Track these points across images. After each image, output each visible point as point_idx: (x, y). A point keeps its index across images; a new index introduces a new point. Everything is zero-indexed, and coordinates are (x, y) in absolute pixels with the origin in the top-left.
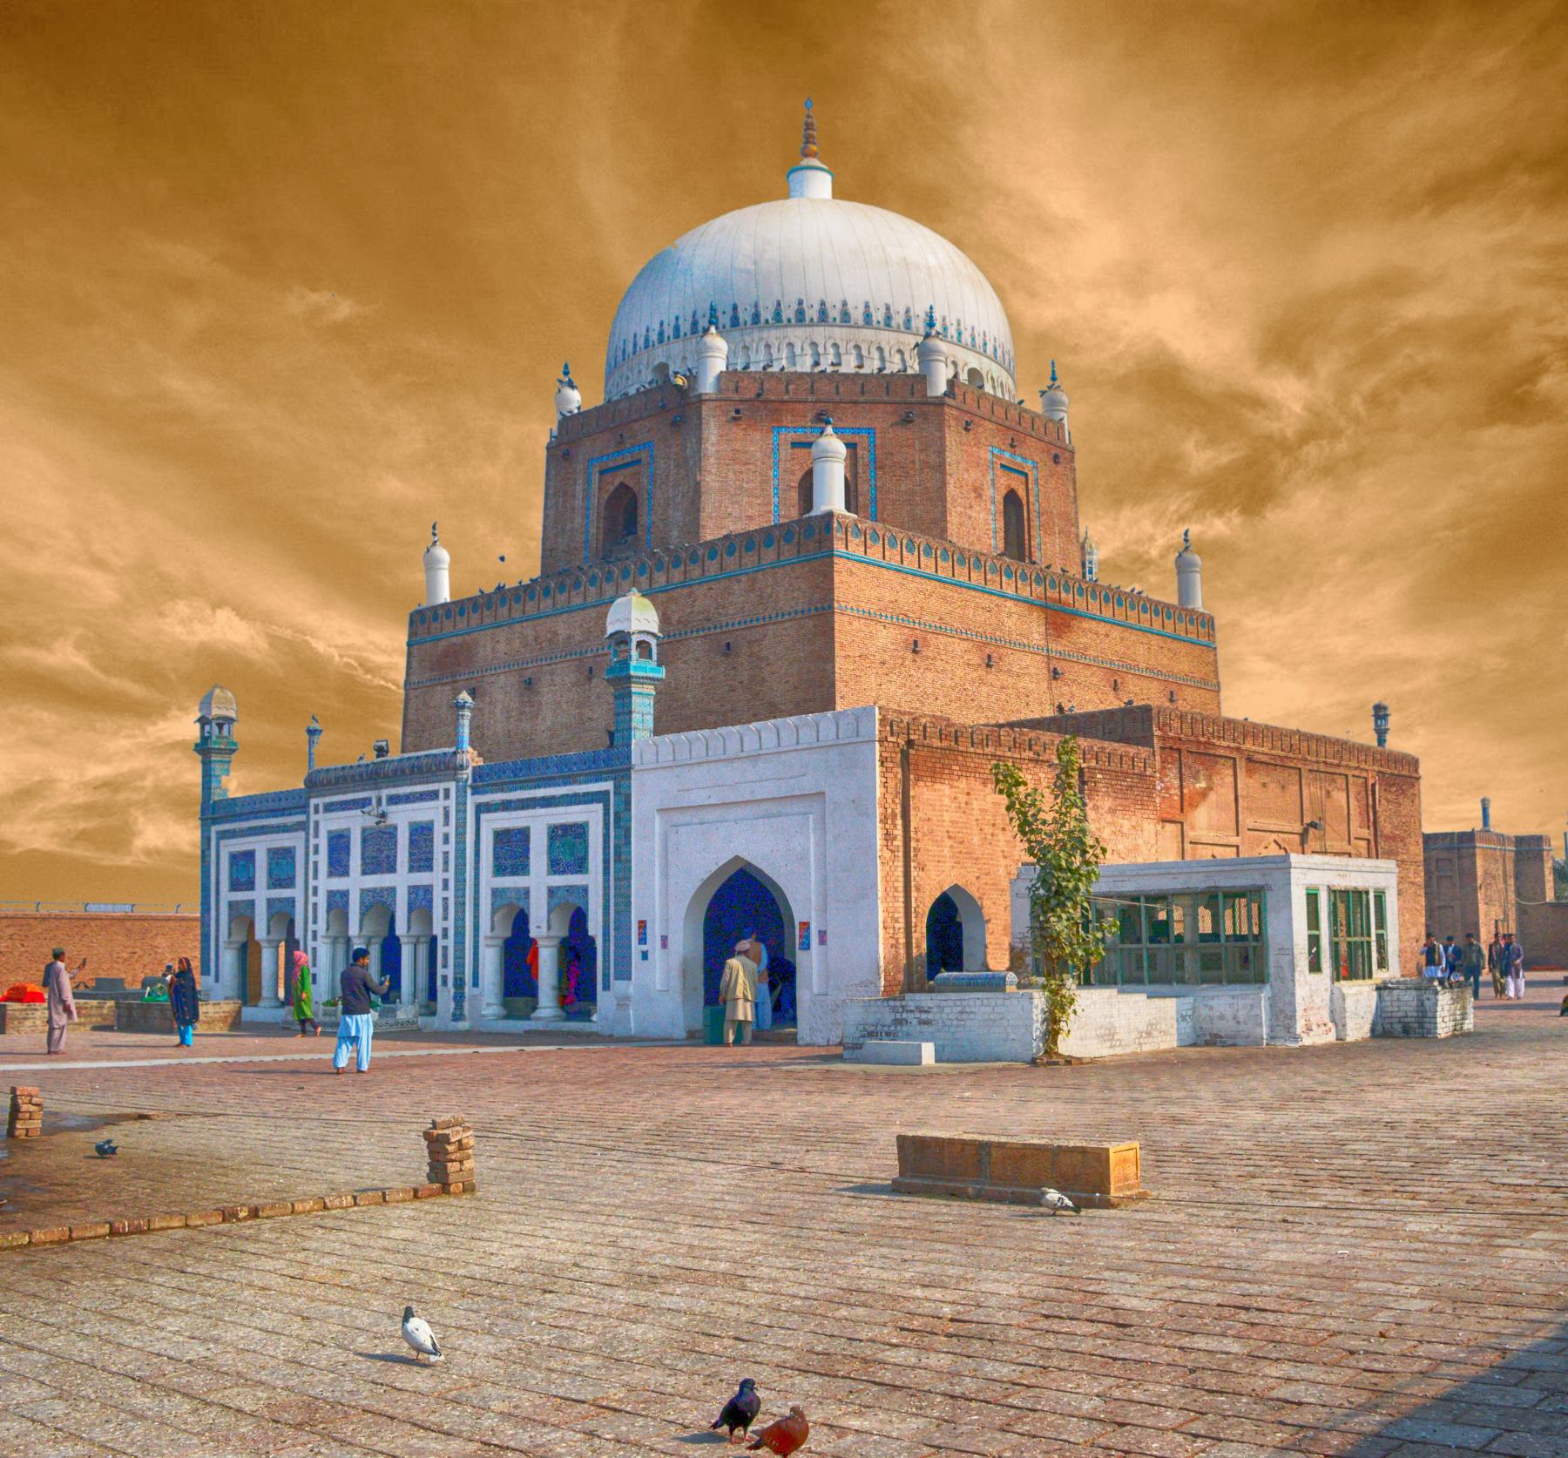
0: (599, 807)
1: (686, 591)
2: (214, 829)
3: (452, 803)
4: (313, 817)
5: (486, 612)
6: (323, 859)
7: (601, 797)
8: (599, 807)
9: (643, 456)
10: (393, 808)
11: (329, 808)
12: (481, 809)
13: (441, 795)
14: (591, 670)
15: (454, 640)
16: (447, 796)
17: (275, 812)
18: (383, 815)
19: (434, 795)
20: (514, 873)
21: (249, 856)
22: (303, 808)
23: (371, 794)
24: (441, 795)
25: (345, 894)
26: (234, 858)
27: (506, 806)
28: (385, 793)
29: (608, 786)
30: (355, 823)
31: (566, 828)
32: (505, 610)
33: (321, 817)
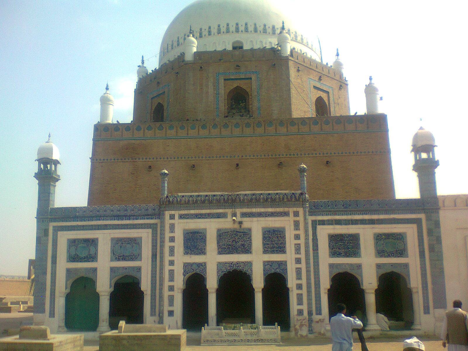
0: (415, 226)
1: (299, 136)
2: (52, 224)
3: (301, 218)
4: (168, 221)
5: (158, 131)
6: (179, 244)
7: (418, 222)
8: (415, 226)
9: (254, 78)
10: (245, 219)
11: (181, 217)
12: (315, 224)
13: (291, 214)
14: (237, 165)
15: (133, 141)
16: (296, 214)
17: (118, 217)
18: (240, 223)
19: (286, 214)
20: (347, 255)
21: (93, 242)
22: (159, 215)
23: (229, 211)
24: (291, 214)
25: (203, 266)
26: (73, 243)
27: (338, 222)
28: (238, 211)
29: (422, 216)
30: (211, 227)
31: (388, 236)
32: (173, 132)
33: (176, 221)
